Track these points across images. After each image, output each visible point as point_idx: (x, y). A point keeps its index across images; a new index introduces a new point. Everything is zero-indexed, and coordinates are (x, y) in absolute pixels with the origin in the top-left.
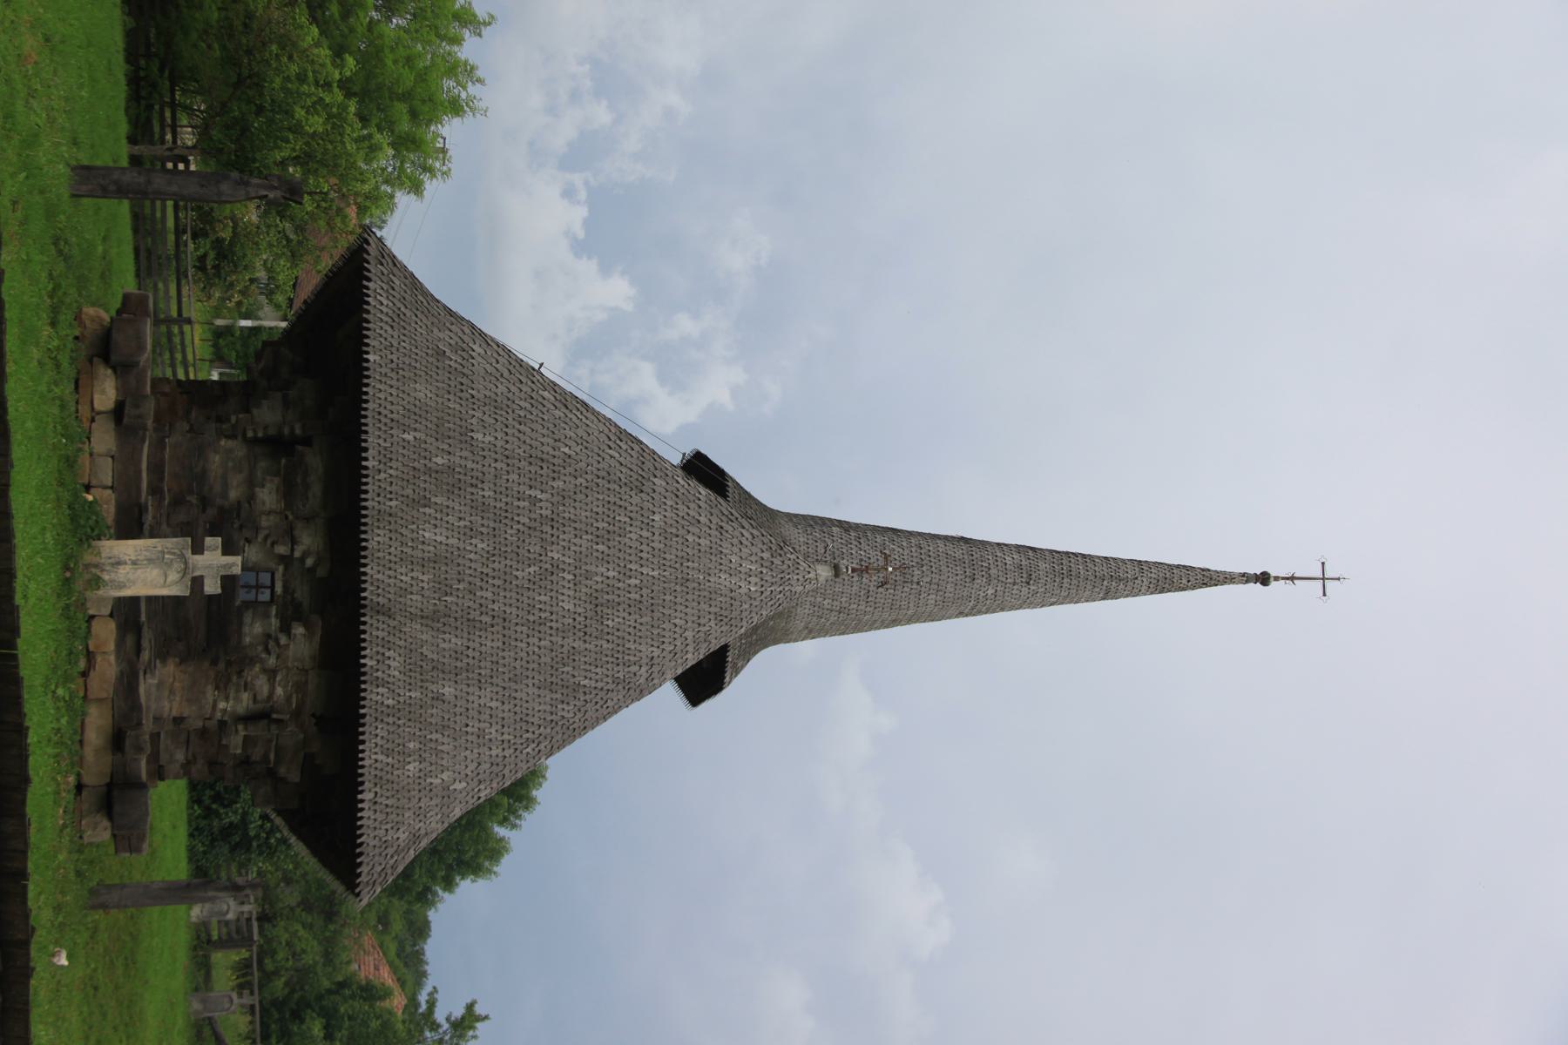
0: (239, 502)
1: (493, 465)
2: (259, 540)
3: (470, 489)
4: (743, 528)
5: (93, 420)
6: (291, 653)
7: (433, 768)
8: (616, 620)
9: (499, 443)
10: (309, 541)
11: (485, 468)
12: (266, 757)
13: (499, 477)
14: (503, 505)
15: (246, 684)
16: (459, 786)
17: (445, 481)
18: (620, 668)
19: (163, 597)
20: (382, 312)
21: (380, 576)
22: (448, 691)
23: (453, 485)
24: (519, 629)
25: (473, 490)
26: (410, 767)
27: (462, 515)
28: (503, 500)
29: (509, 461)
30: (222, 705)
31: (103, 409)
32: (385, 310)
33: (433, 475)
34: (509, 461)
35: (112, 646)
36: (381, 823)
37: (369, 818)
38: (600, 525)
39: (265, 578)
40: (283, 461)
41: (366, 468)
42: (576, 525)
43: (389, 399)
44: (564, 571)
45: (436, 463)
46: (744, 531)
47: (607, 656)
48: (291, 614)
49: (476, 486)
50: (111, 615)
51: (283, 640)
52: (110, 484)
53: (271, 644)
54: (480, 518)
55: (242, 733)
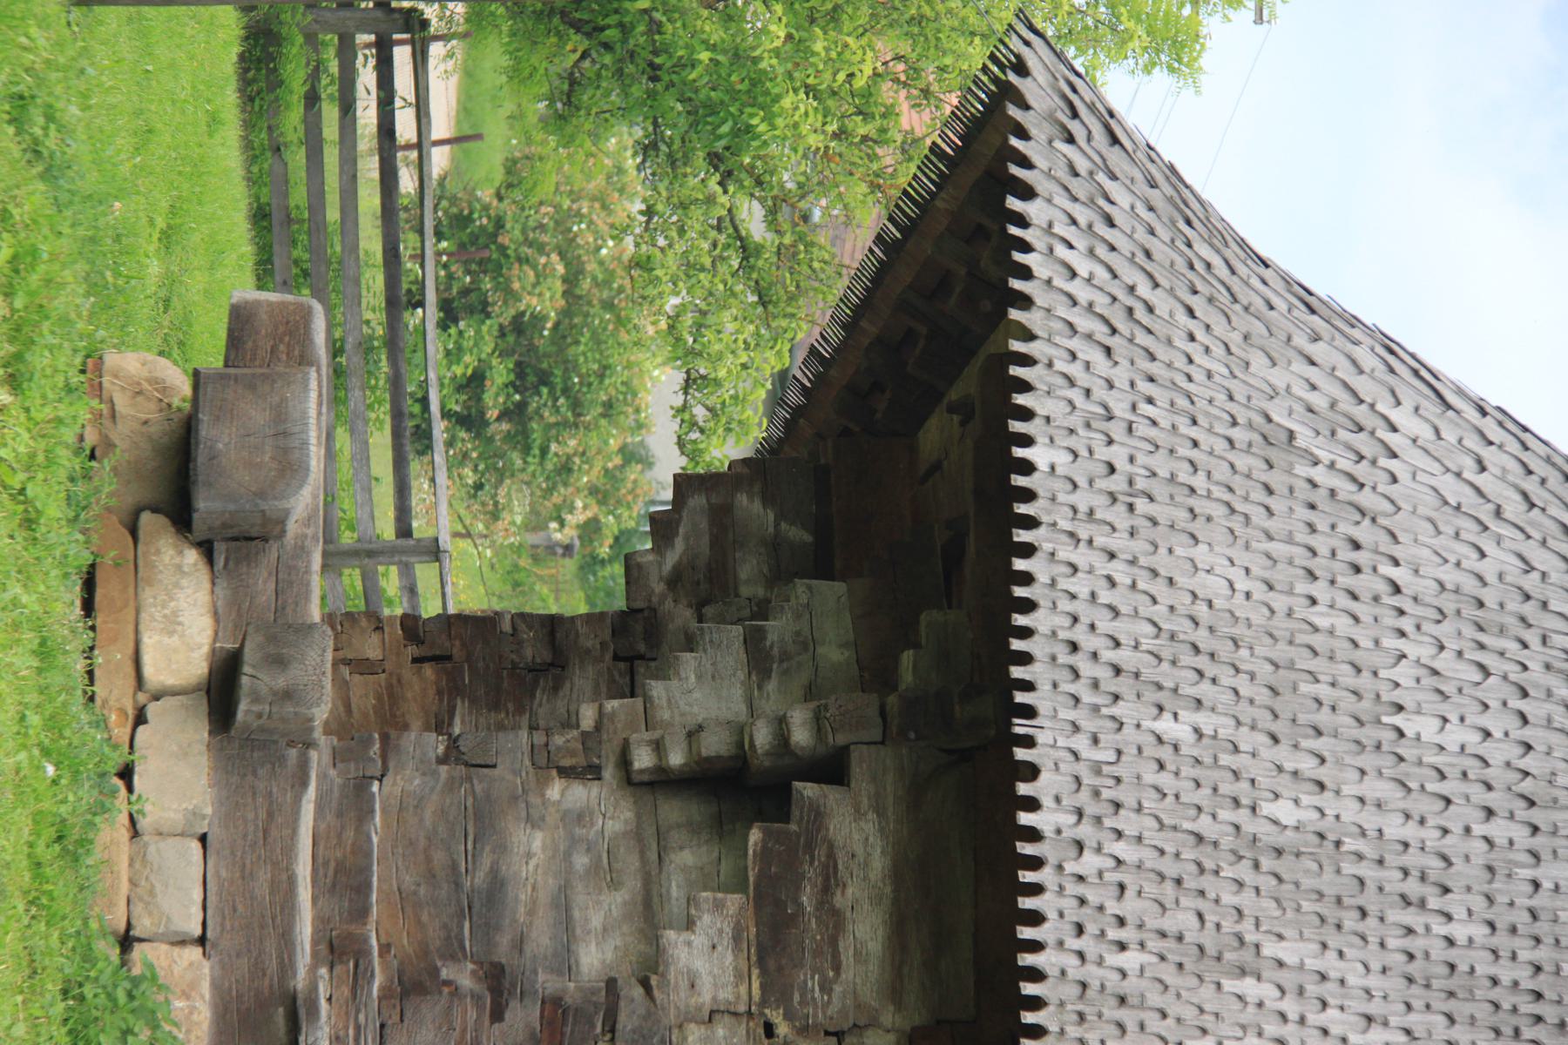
1: (1478, 829)
11: (1449, 839)
13: (1501, 872)
14: (1523, 974)
17: (1307, 883)
23: (1339, 901)
25: (1411, 917)
27: (1374, 1008)
28: (1524, 955)
33: (1267, 863)
34: (1536, 816)
45: (1275, 822)
49: (1422, 904)
54: (1441, 1019)
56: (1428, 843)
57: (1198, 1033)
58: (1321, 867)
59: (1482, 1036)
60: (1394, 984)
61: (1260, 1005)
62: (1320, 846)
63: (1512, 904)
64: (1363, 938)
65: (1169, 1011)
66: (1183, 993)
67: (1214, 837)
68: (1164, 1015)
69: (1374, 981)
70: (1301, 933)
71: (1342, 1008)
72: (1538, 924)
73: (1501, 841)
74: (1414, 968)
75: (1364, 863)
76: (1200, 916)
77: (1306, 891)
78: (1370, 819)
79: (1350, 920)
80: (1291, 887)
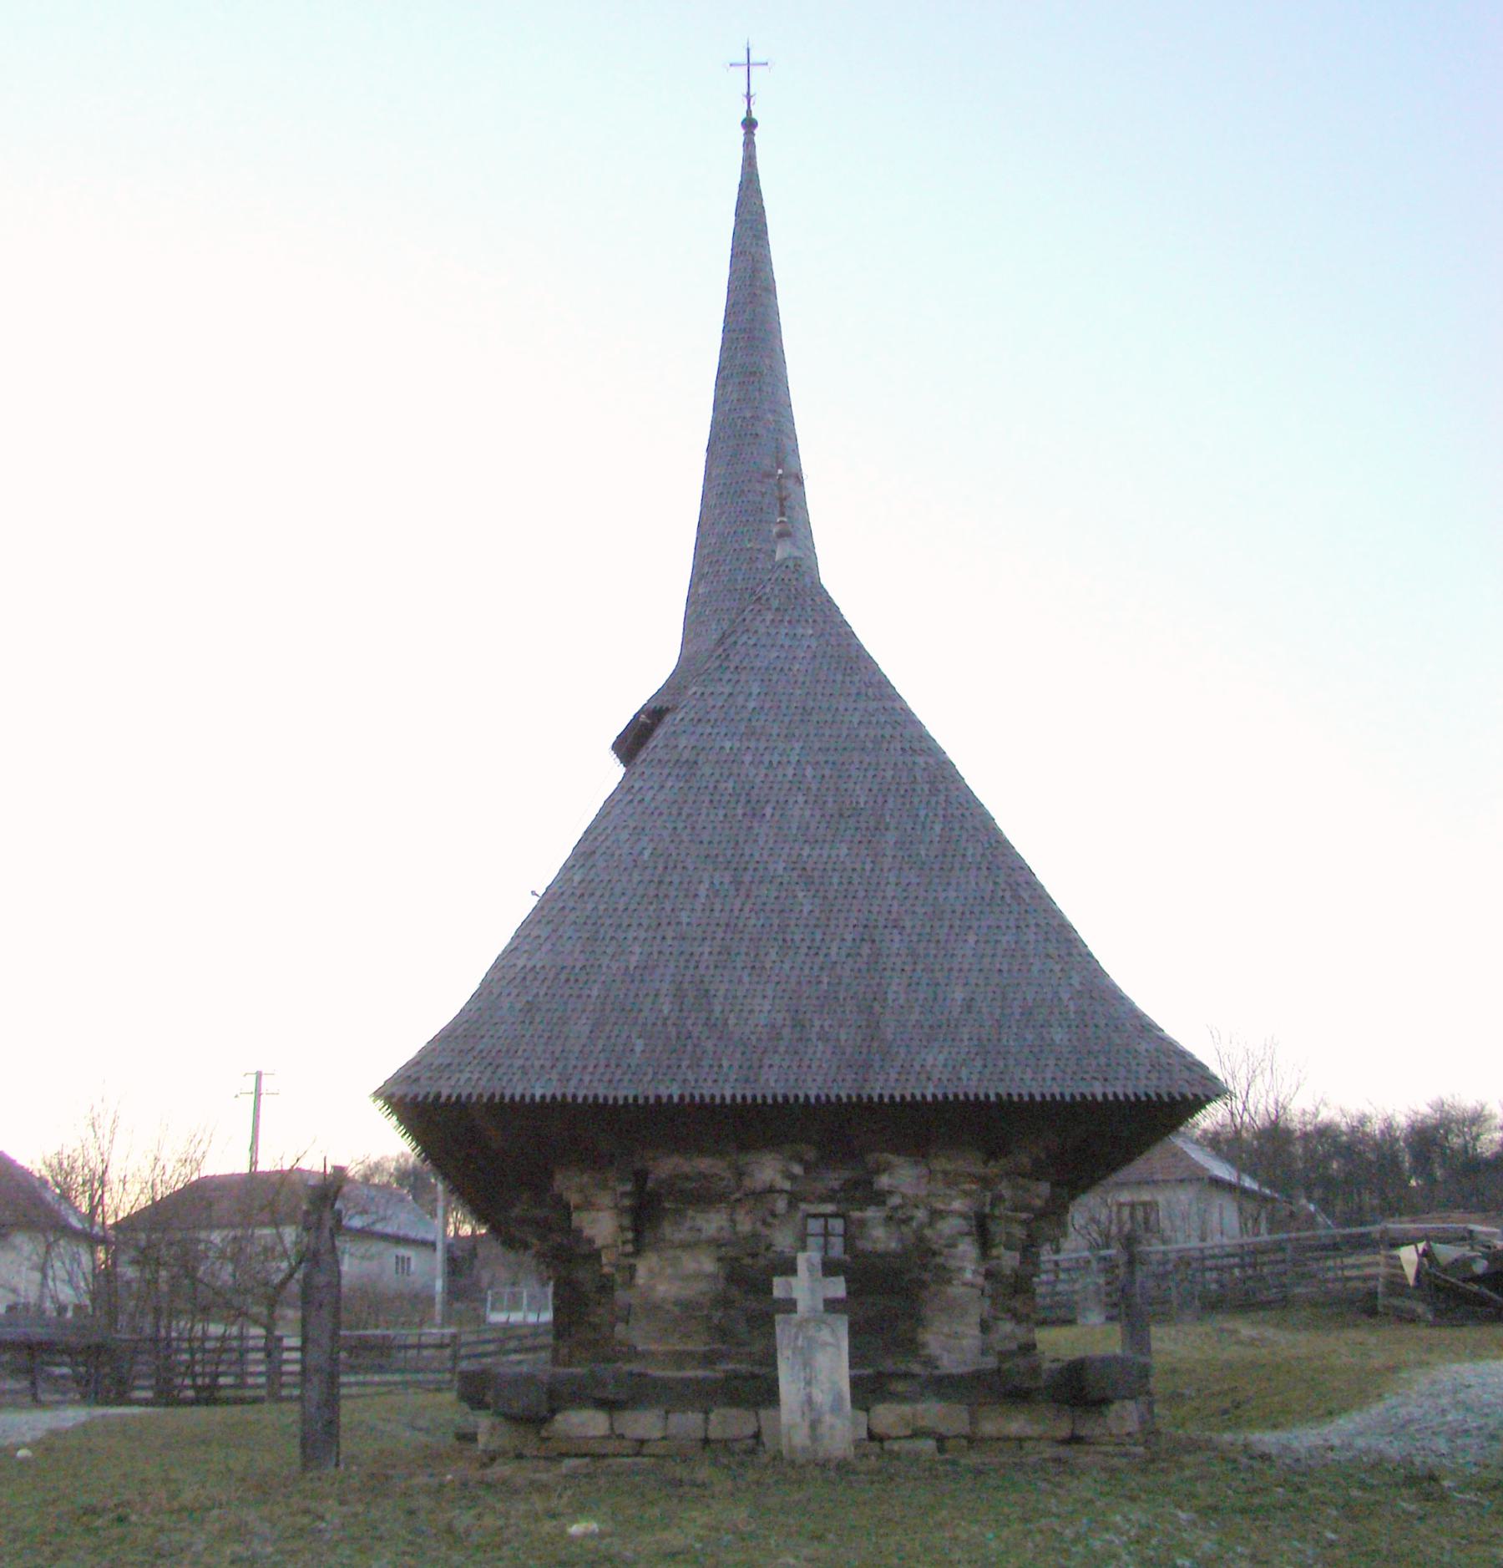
0: (720, 1259)
2: (768, 1233)
3: (702, 971)
4: (735, 643)
5: (622, 1437)
6: (910, 1192)
7: (1056, 1011)
8: (858, 792)
9: (642, 935)
10: (768, 1170)
12: (1024, 1222)
15: (948, 1246)
16: (1076, 981)
18: (918, 788)
19: (850, 1346)
20: (479, 1079)
21: (820, 1079)
22: (959, 994)
24: (875, 909)
25: (702, 966)
26: (1057, 1038)
30: (968, 1275)
31: (607, 1425)
32: (476, 1076)
33: (685, 1014)
35: (906, 1409)
36: (1129, 1071)
37: (1125, 1086)
38: (740, 811)
39: (815, 1226)
40: (667, 1205)
41: (682, 1097)
42: (741, 840)
43: (590, 1069)
44: (799, 855)
46: (740, 643)
47: (904, 804)
48: (864, 1192)
50: (867, 1410)
51: (895, 1200)
52: (701, 1416)
53: (900, 1214)
55: (1002, 1249)
69: (726, 979)
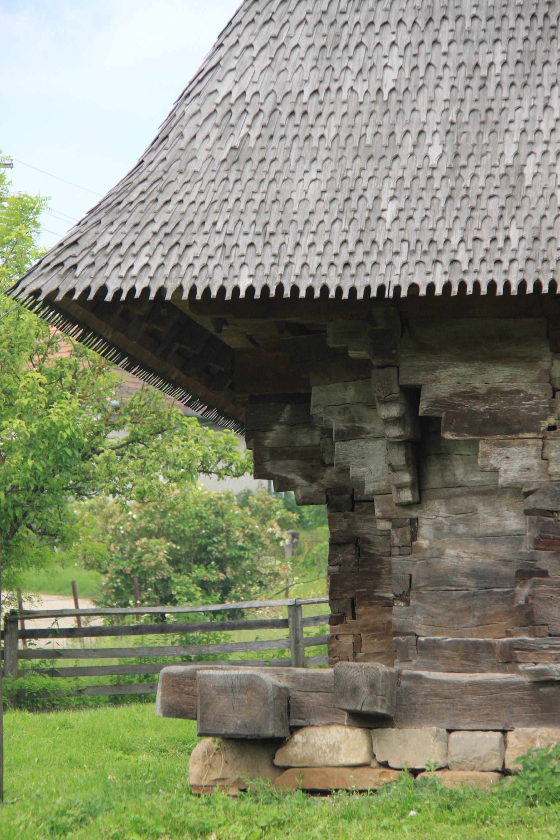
1: (444, 48)
3: (491, 91)
11: (450, 64)
13: (467, 36)
14: (522, 24)
17: (473, 140)
23: (483, 123)
25: (492, 84)
27: (540, 104)
28: (512, 24)
29: (437, 17)
33: (463, 162)
34: (437, 17)
45: (441, 157)
49: (484, 78)
54: (547, 68)
56: (452, 75)
57: (554, 198)
58: (464, 132)
59: (555, 47)
60: (527, 93)
61: (538, 165)
62: (453, 133)
63: (484, 30)
64: (503, 110)
65: (542, 214)
66: (532, 206)
67: (448, 190)
68: (544, 216)
69: (526, 104)
70: (500, 143)
71: (540, 121)
72: (495, 16)
73: (451, 36)
74: (519, 82)
75: (463, 109)
76: (491, 197)
77: (478, 140)
78: (439, 106)
79: (494, 117)
80: (475, 148)
